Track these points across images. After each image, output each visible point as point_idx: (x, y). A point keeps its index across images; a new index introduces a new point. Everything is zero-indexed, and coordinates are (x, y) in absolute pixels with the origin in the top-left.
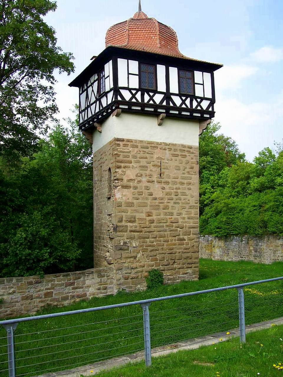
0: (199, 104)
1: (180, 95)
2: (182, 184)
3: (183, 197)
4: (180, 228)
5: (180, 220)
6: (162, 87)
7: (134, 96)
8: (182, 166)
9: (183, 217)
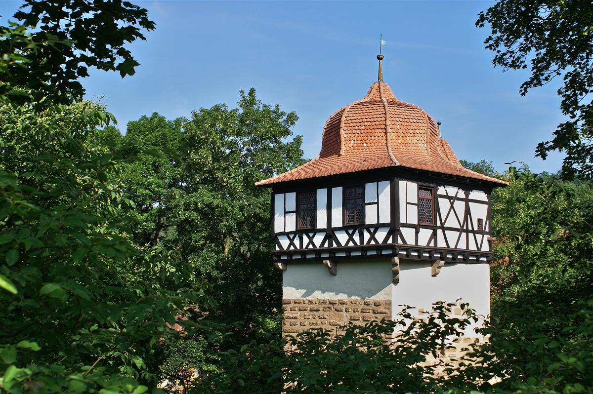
0: (373, 237)
1: (345, 228)
6: (321, 223)
7: (292, 243)
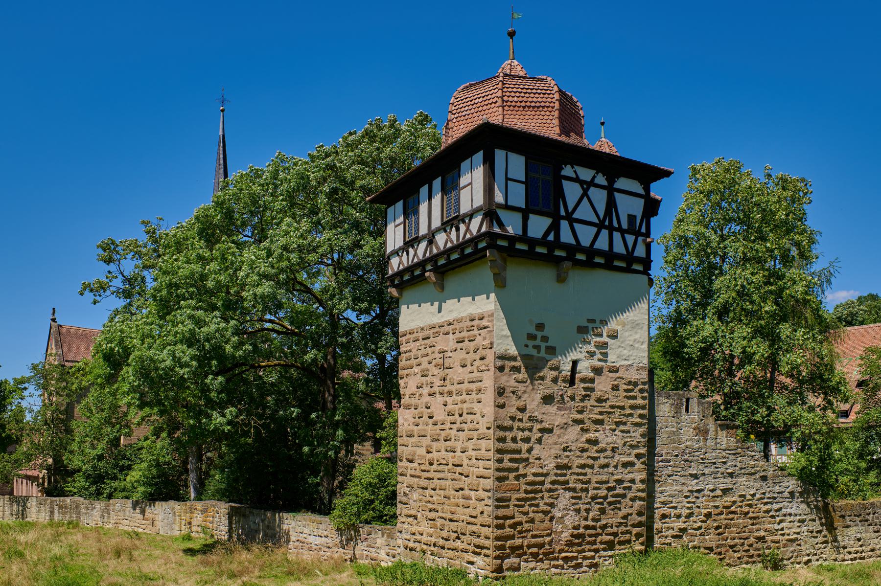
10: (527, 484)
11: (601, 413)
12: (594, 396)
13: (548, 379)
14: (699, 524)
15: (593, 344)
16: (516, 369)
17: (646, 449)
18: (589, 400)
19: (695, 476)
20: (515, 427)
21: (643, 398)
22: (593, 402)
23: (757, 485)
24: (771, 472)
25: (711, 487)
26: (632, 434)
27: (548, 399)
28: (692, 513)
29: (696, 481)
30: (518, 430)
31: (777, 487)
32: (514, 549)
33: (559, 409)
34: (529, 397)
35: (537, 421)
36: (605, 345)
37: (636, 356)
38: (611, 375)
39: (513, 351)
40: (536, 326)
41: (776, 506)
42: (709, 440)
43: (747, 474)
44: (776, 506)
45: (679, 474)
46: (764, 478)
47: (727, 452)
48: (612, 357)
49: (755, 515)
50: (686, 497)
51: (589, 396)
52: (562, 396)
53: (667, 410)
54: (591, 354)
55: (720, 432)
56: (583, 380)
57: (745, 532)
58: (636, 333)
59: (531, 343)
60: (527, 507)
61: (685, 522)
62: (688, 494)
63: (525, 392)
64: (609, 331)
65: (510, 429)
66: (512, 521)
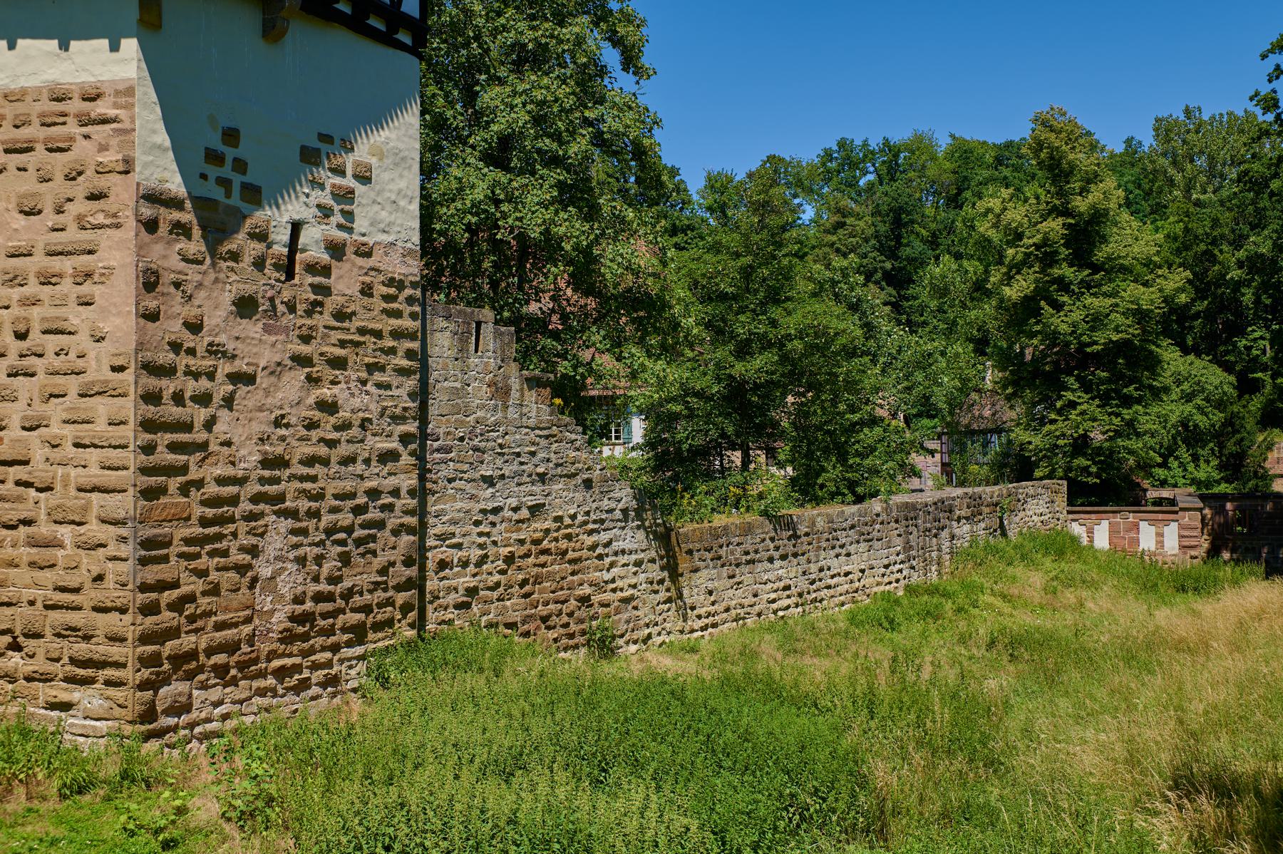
2: (47, 280)
3: (53, 342)
4: (40, 490)
5: (39, 454)
8: (49, 195)
9: (56, 437)
10: (204, 503)
11: (342, 344)
12: (331, 303)
13: (247, 260)
14: (497, 577)
15: (328, 189)
16: (181, 229)
17: (417, 424)
18: (321, 313)
19: (489, 481)
20: (181, 369)
21: (413, 316)
22: (326, 319)
23: (579, 496)
24: (598, 472)
25: (513, 502)
26: (395, 392)
27: (245, 306)
28: (486, 556)
29: (490, 490)
30: (186, 374)
31: (606, 502)
32: (178, 660)
33: (267, 330)
34: (209, 297)
35: (224, 354)
36: (345, 196)
37: (402, 225)
38: (360, 261)
39: (176, 185)
40: (224, 134)
41: (604, 537)
42: (510, 409)
43: (566, 476)
44: (604, 537)
45: (466, 476)
46: (588, 484)
47: (537, 432)
48: (360, 224)
49: (576, 555)
50: (477, 523)
51: (321, 304)
52: (272, 299)
53: (446, 344)
54: (326, 212)
55: (527, 393)
56: (312, 268)
57: (562, 589)
58: (401, 176)
59: (213, 172)
60: (205, 558)
61: (474, 575)
62: (480, 517)
63: (200, 285)
64: (357, 164)
65: (168, 371)
66: (175, 594)
